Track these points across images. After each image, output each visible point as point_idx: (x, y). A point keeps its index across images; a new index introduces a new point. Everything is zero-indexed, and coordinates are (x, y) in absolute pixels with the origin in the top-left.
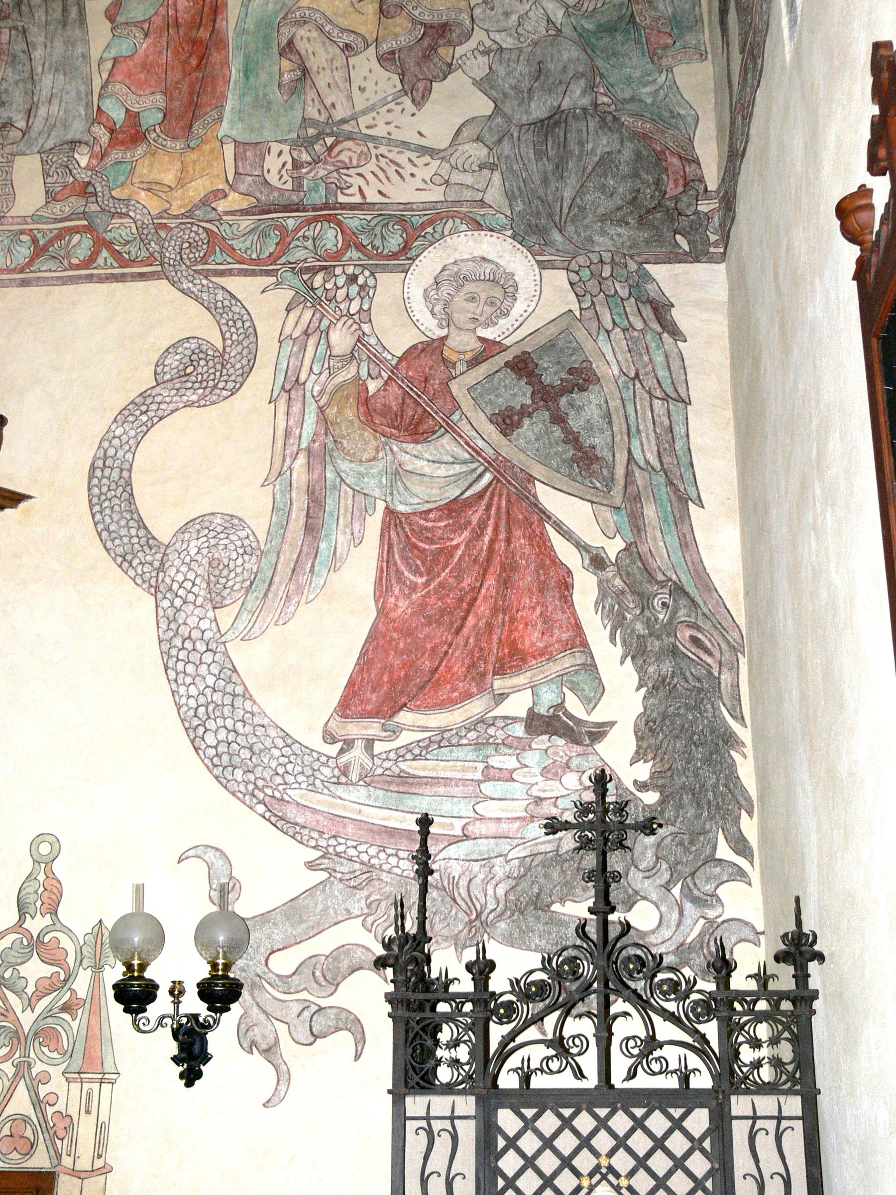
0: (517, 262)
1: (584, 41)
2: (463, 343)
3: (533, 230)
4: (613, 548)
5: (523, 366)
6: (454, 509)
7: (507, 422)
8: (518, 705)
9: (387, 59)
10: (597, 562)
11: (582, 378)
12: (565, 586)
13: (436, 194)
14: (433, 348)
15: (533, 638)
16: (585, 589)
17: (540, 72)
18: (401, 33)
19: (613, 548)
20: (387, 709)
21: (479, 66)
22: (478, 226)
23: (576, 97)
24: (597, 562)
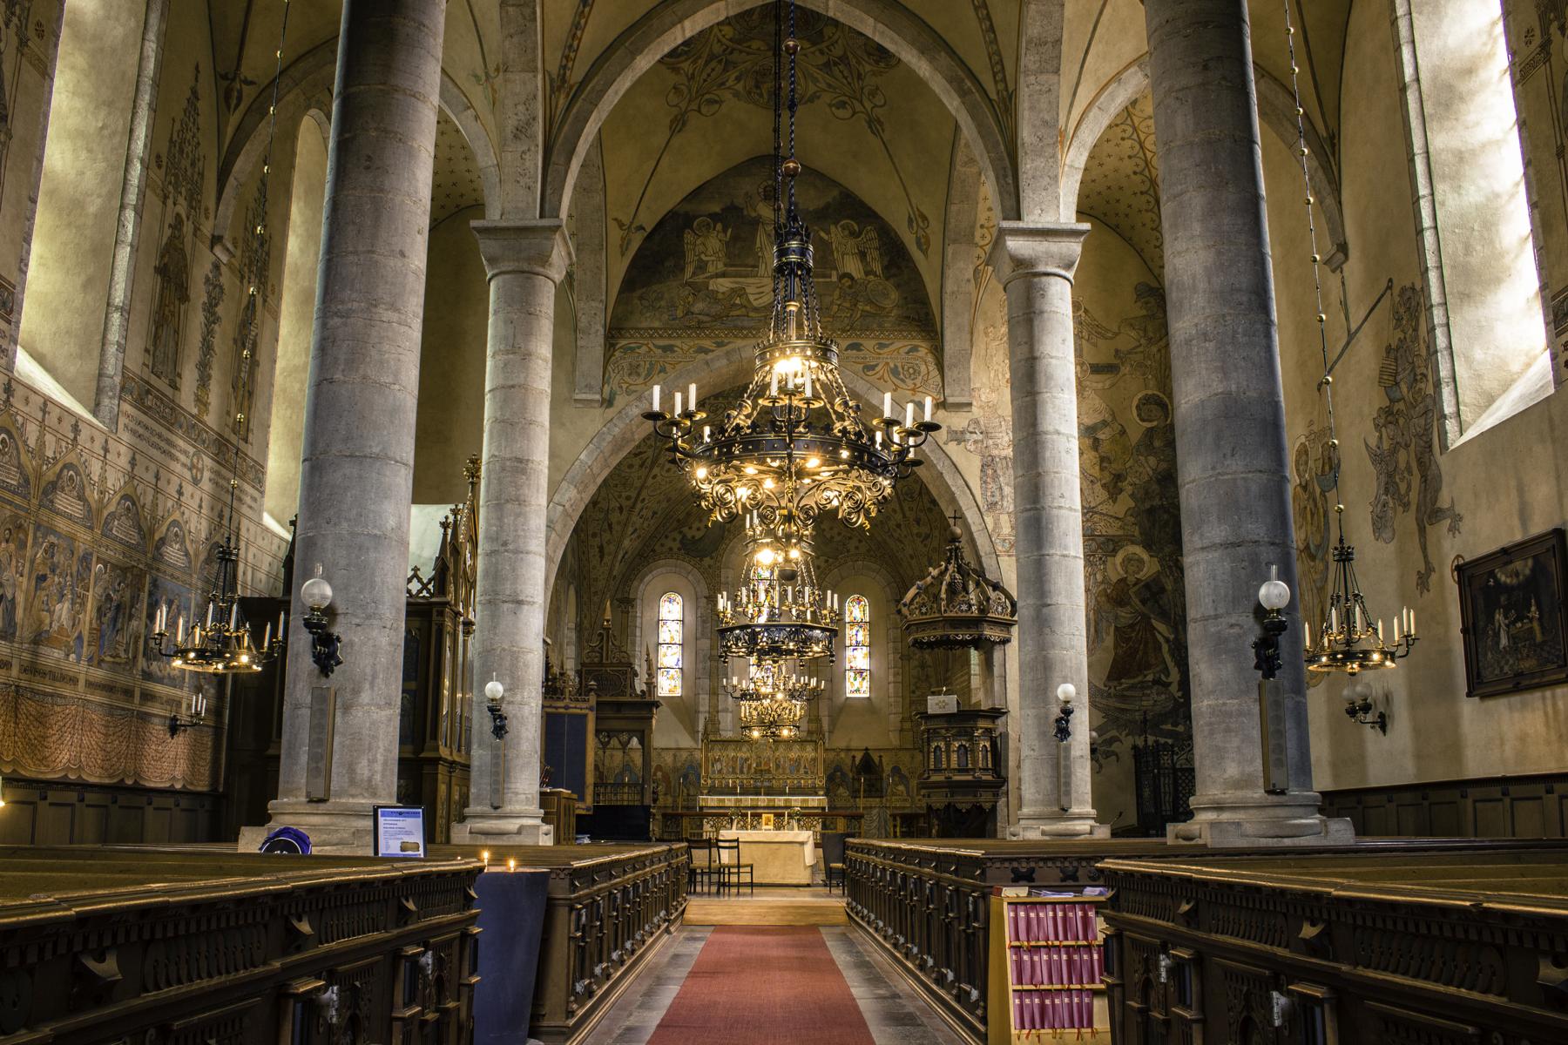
0: (1145, 556)
1: (1159, 482)
2: (1131, 580)
3: (1148, 546)
4: (1172, 637)
5: (1147, 586)
6: (1131, 626)
7: (1144, 602)
8: (1150, 678)
9: (1104, 486)
10: (1167, 640)
11: (1163, 590)
12: (1160, 648)
13: (1120, 533)
14: (1123, 580)
15: (1153, 661)
16: (1165, 648)
17: (1147, 493)
18: (1107, 478)
19: (1172, 637)
20: (1119, 679)
21: (1129, 489)
22: (1133, 543)
23: (1157, 502)
24: (1167, 640)
